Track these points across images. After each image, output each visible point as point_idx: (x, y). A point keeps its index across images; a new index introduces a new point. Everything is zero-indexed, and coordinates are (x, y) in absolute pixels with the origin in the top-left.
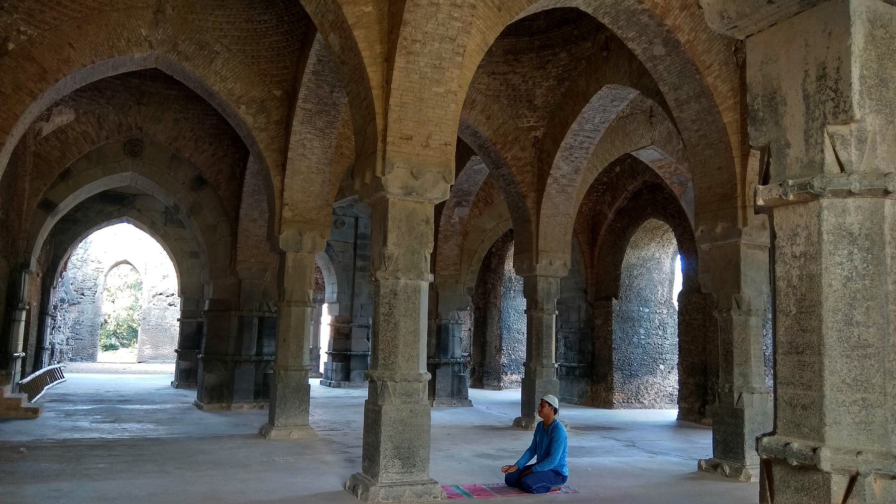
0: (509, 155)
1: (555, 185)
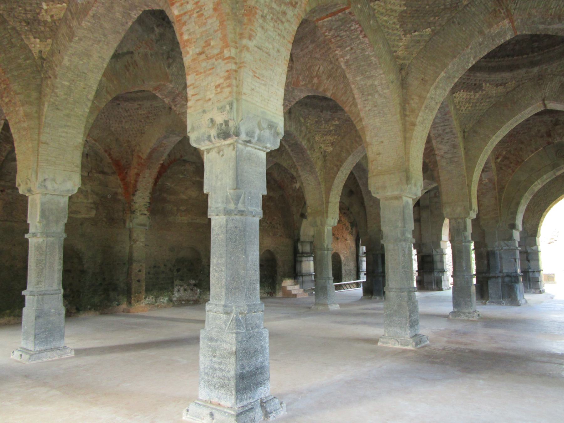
1: (443, 160)
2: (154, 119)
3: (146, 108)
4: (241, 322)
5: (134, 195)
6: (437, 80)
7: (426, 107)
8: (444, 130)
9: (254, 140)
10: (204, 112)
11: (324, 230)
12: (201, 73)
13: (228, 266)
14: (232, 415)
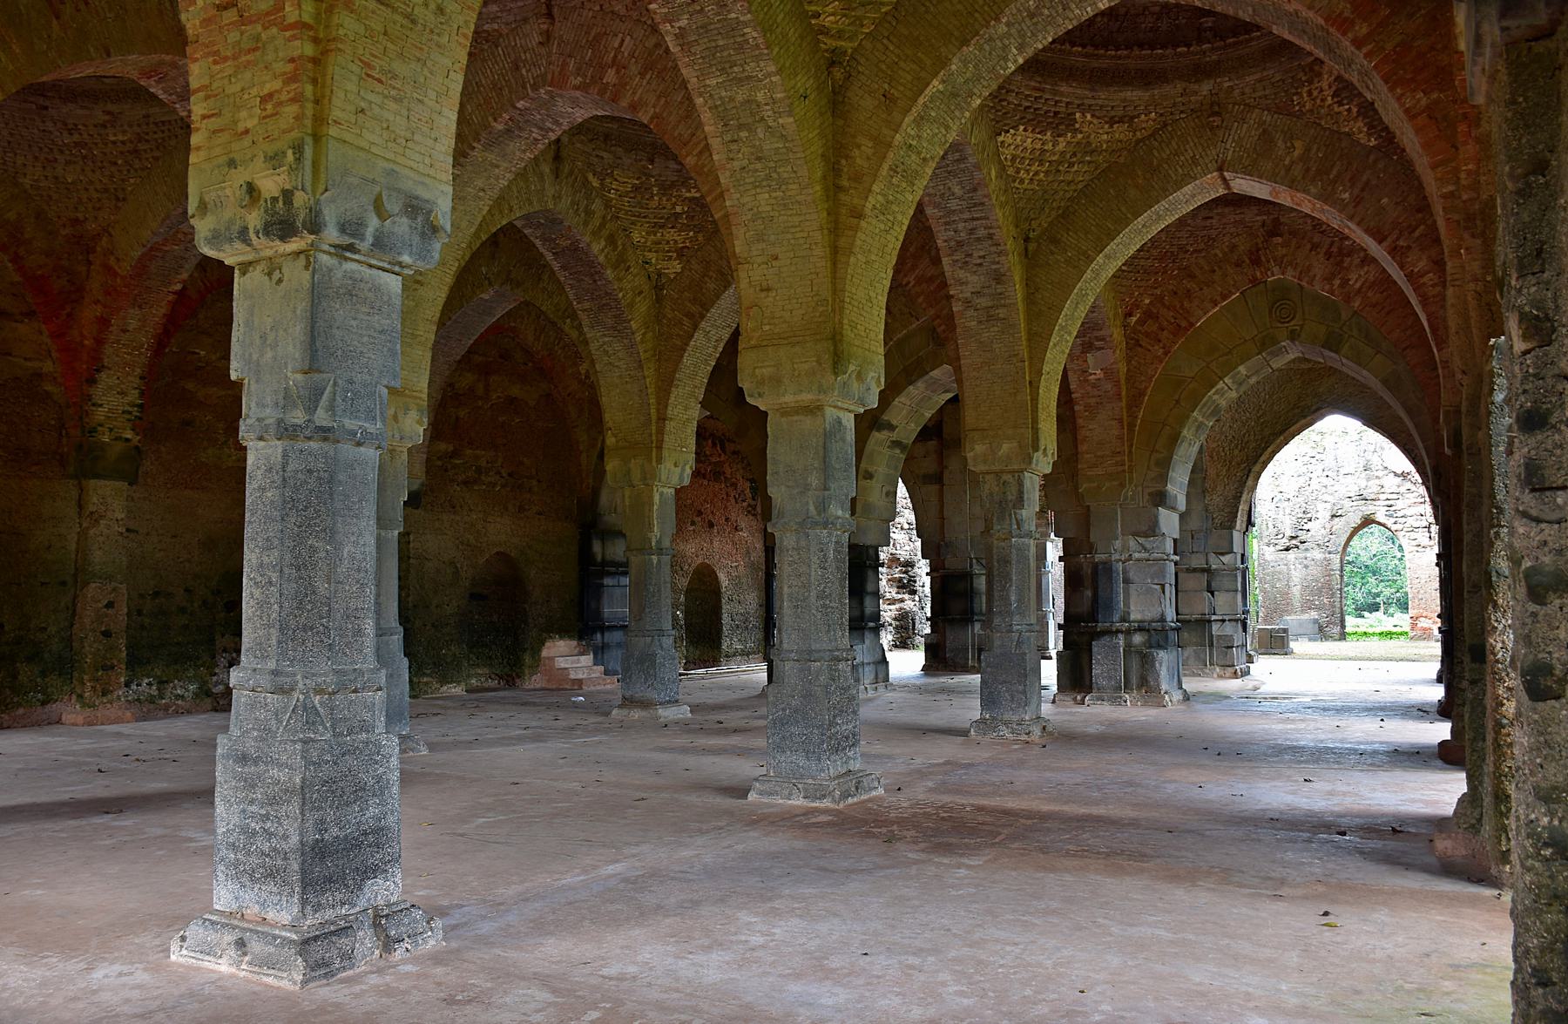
0: (911, 279)
1: (971, 312)
2: (156, 159)
3: (131, 126)
4: (318, 714)
5: (92, 381)
6: (921, 100)
7: (893, 170)
8: (972, 231)
9: (364, 246)
10: (232, 164)
11: (651, 497)
12: (226, 59)
13: (286, 570)
14: (292, 941)
